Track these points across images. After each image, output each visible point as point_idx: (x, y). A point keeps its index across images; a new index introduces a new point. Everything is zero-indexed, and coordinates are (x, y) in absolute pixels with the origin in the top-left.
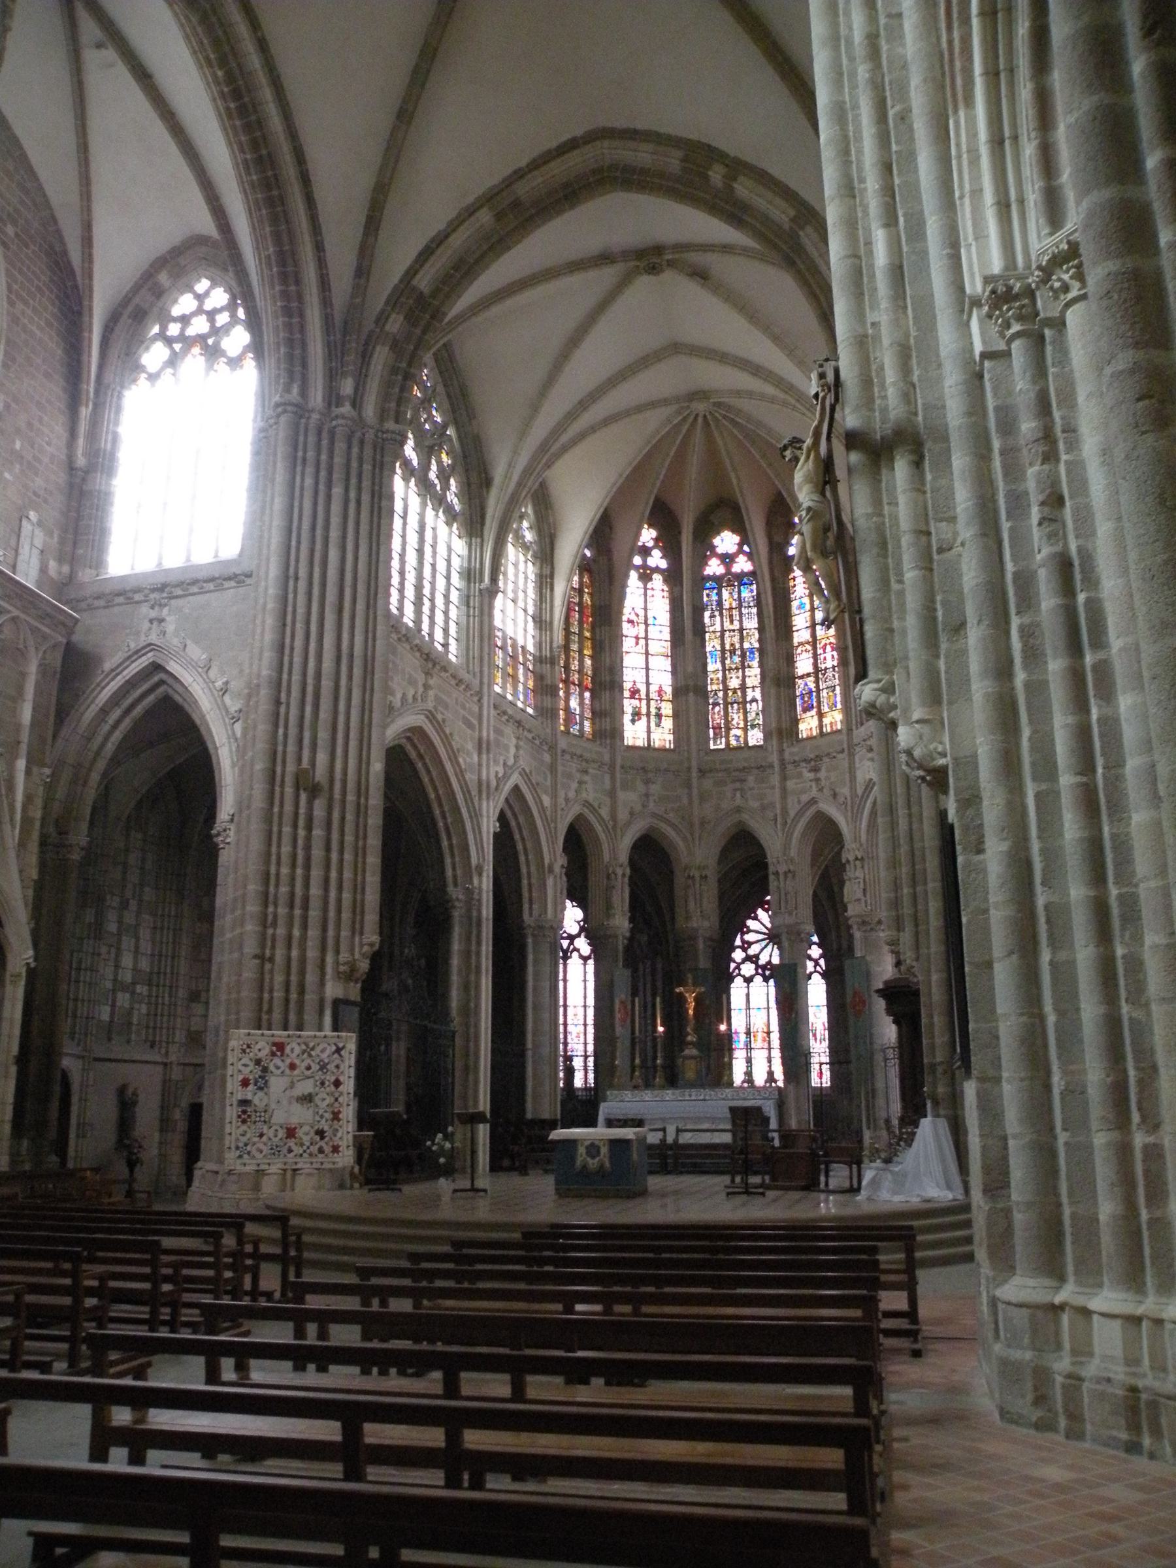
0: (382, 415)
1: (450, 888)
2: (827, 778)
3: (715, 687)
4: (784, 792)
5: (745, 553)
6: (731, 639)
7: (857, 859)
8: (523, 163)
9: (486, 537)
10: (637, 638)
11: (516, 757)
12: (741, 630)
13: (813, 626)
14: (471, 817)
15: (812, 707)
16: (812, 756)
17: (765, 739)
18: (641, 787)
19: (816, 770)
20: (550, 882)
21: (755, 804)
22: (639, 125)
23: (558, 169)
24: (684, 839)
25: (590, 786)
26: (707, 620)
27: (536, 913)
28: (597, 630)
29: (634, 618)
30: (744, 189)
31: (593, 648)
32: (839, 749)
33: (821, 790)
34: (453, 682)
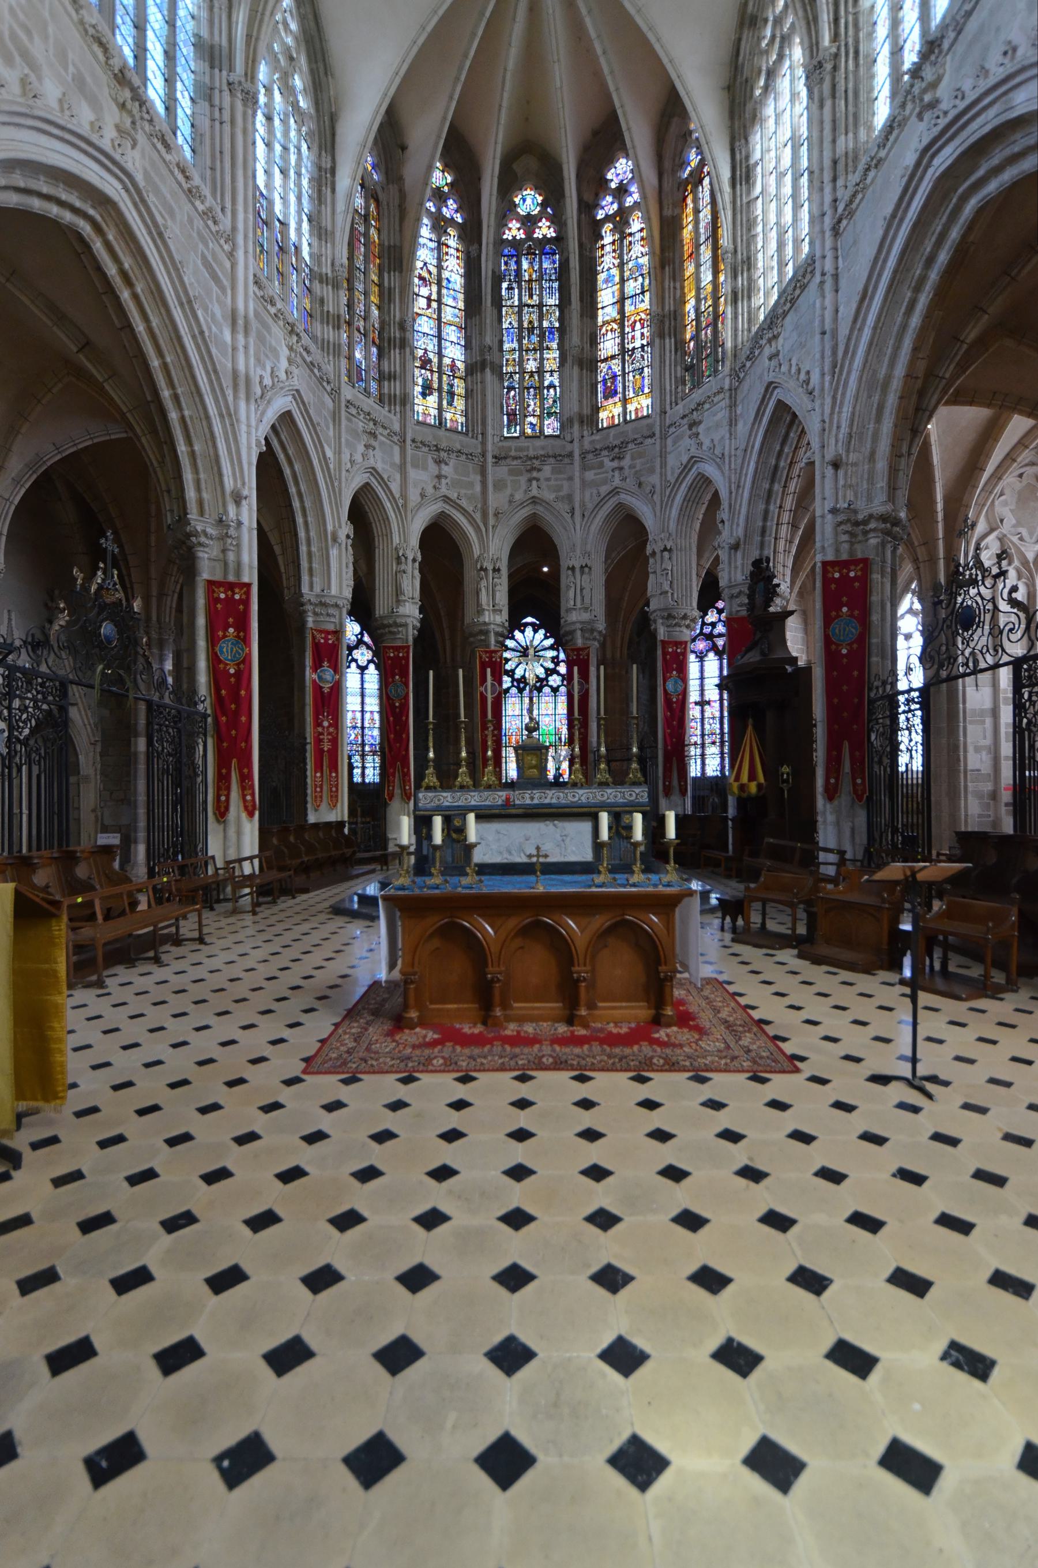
1: (193, 515)
2: (631, 467)
3: (510, 369)
4: (584, 483)
6: (529, 316)
10: (429, 299)
12: (540, 306)
15: (615, 393)
16: (617, 442)
17: (562, 428)
20: (334, 552)
24: (477, 529)
25: (378, 453)
26: (503, 293)
27: (317, 589)
28: (386, 275)
29: (425, 274)
31: (381, 295)
32: (646, 433)
33: (624, 479)
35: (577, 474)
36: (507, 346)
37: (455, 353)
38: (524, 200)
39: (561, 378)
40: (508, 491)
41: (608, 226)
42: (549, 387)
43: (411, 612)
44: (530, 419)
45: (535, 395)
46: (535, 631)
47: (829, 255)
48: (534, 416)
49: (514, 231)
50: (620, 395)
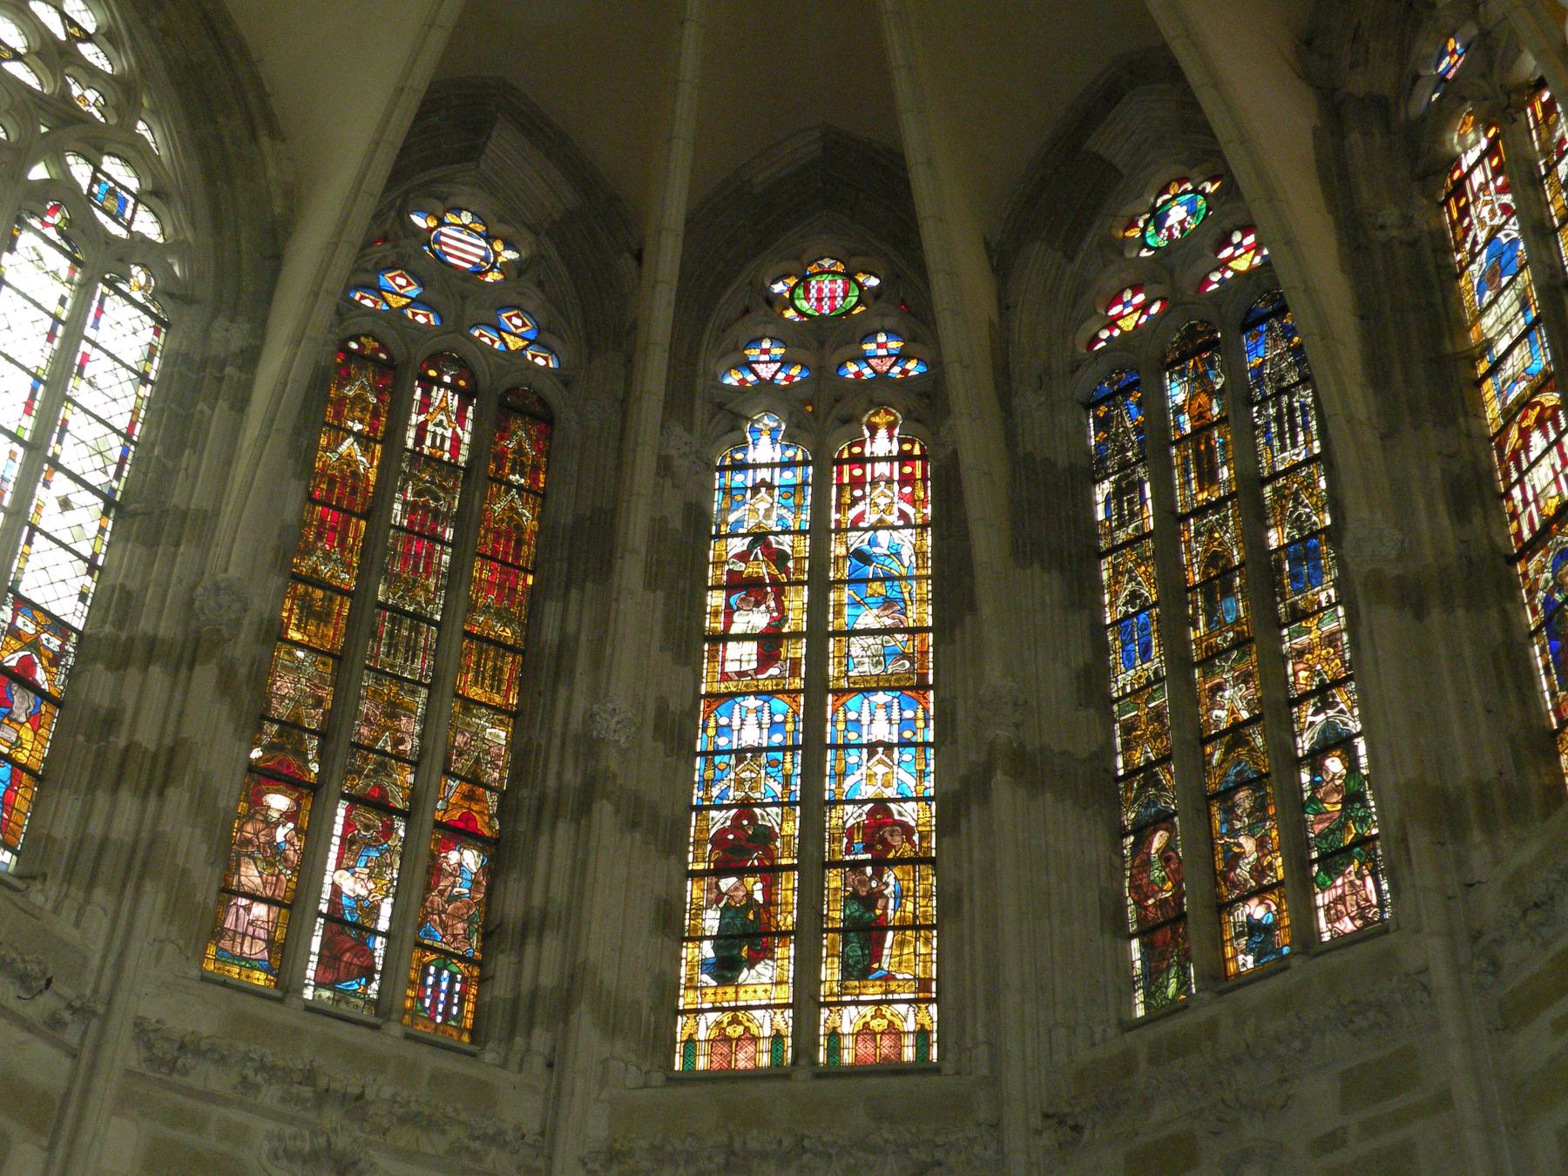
10: (770, 642)
44: (1256, 910)
45: (1259, 808)
48: (1260, 892)
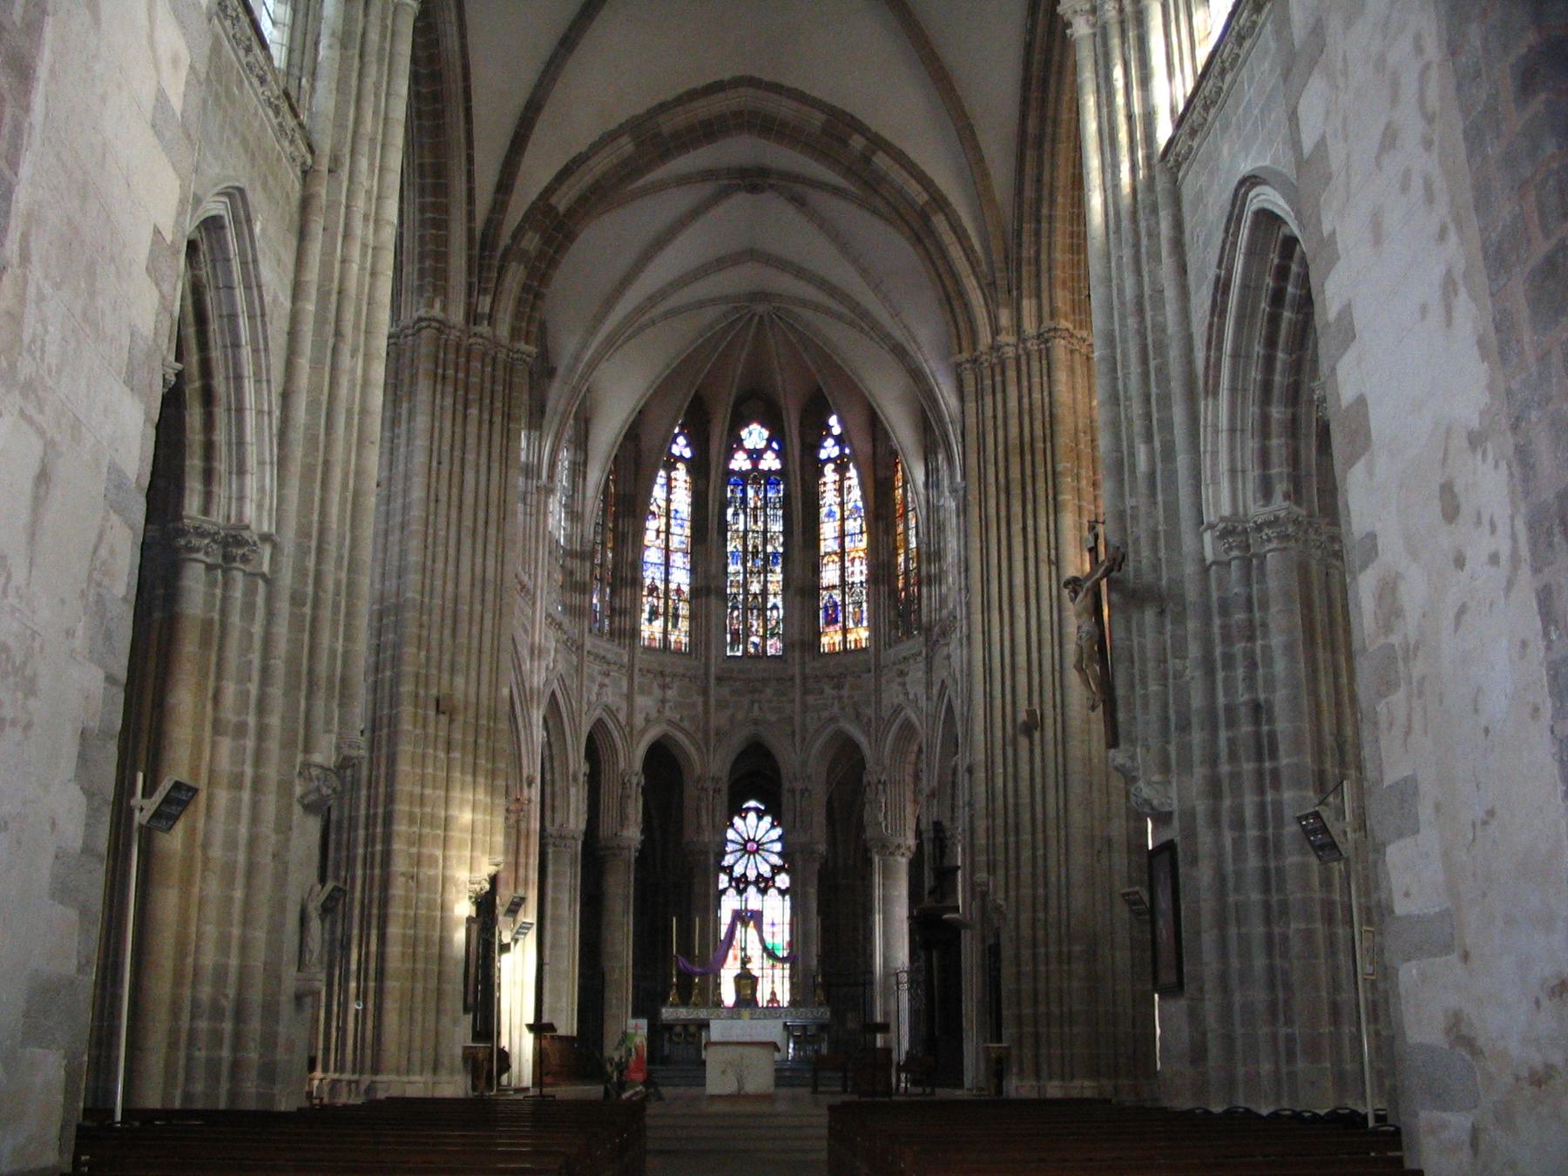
0: (515, 333)
2: (850, 697)
3: (734, 590)
4: (805, 708)
5: (774, 450)
7: (879, 782)
8: (669, 96)
9: (545, 431)
10: (658, 532)
11: (555, 661)
12: (765, 531)
13: (842, 535)
14: (525, 727)
15: (836, 621)
17: (785, 649)
18: (657, 692)
19: (839, 687)
20: (573, 790)
21: (773, 718)
22: (787, 82)
23: (703, 109)
24: (698, 749)
26: (729, 518)
27: (558, 822)
29: (653, 508)
30: (881, 161)
31: (615, 539)
33: (843, 708)
34: (519, 587)
35: (797, 699)
36: (731, 569)
37: (681, 577)
38: (750, 433)
39: (784, 600)
40: (729, 712)
41: (829, 468)
42: (772, 609)
43: (633, 834)
46: (760, 818)
47: (964, 622)
49: (740, 462)
50: (840, 624)
